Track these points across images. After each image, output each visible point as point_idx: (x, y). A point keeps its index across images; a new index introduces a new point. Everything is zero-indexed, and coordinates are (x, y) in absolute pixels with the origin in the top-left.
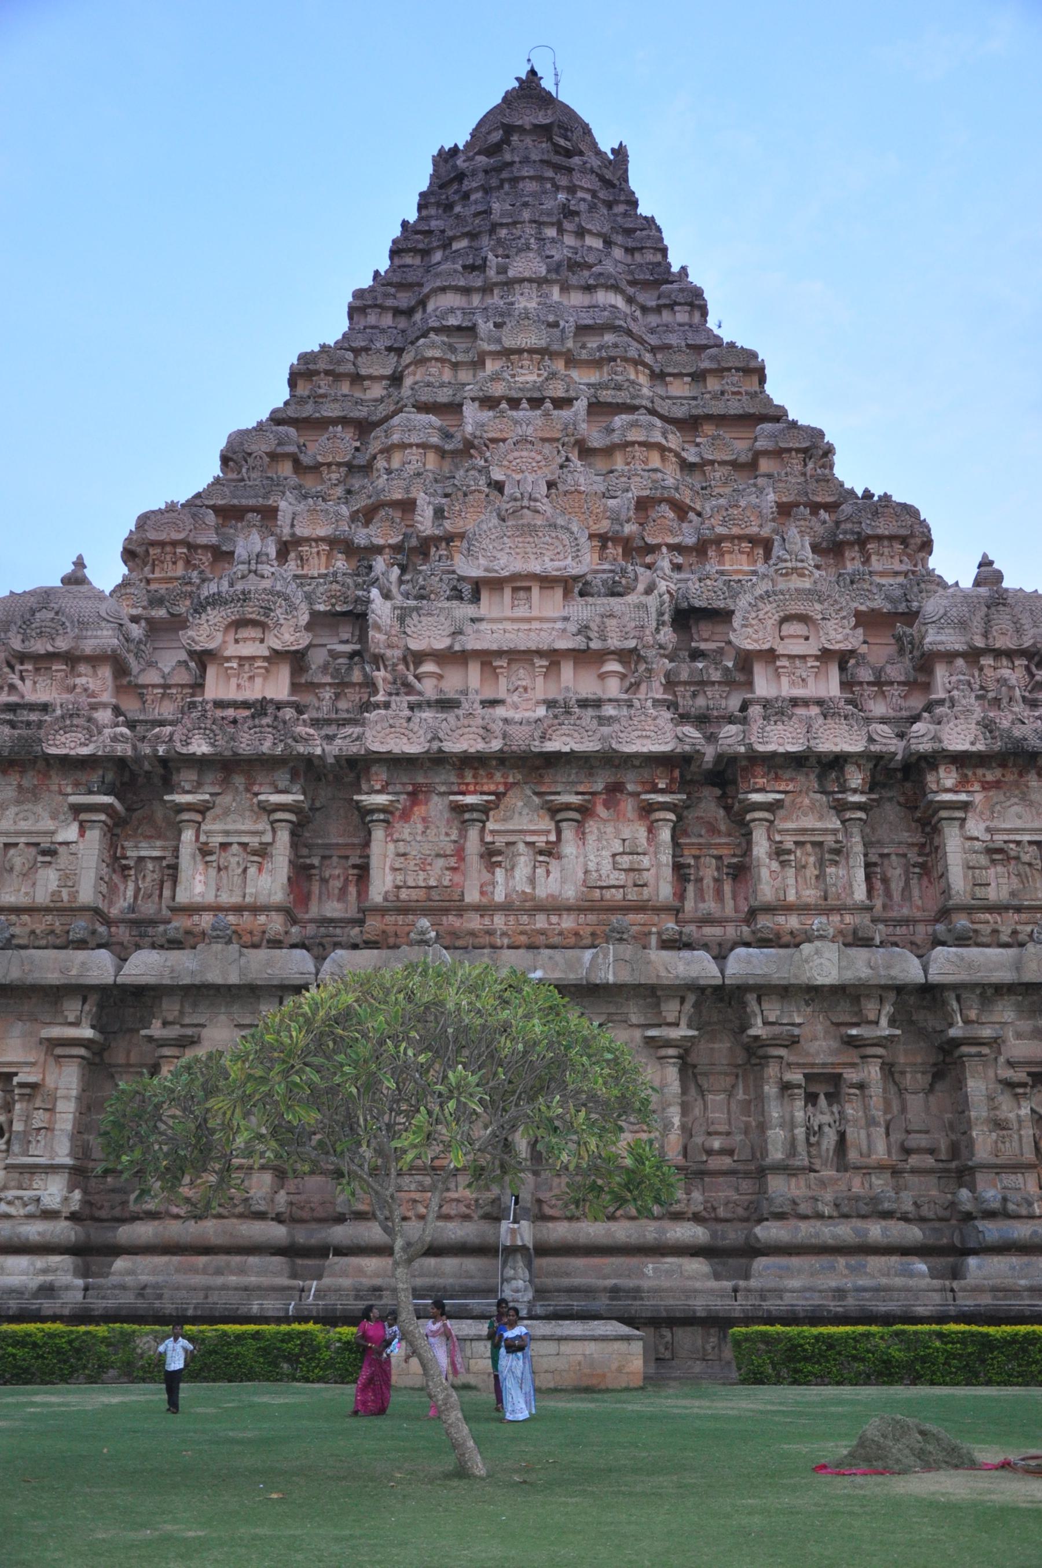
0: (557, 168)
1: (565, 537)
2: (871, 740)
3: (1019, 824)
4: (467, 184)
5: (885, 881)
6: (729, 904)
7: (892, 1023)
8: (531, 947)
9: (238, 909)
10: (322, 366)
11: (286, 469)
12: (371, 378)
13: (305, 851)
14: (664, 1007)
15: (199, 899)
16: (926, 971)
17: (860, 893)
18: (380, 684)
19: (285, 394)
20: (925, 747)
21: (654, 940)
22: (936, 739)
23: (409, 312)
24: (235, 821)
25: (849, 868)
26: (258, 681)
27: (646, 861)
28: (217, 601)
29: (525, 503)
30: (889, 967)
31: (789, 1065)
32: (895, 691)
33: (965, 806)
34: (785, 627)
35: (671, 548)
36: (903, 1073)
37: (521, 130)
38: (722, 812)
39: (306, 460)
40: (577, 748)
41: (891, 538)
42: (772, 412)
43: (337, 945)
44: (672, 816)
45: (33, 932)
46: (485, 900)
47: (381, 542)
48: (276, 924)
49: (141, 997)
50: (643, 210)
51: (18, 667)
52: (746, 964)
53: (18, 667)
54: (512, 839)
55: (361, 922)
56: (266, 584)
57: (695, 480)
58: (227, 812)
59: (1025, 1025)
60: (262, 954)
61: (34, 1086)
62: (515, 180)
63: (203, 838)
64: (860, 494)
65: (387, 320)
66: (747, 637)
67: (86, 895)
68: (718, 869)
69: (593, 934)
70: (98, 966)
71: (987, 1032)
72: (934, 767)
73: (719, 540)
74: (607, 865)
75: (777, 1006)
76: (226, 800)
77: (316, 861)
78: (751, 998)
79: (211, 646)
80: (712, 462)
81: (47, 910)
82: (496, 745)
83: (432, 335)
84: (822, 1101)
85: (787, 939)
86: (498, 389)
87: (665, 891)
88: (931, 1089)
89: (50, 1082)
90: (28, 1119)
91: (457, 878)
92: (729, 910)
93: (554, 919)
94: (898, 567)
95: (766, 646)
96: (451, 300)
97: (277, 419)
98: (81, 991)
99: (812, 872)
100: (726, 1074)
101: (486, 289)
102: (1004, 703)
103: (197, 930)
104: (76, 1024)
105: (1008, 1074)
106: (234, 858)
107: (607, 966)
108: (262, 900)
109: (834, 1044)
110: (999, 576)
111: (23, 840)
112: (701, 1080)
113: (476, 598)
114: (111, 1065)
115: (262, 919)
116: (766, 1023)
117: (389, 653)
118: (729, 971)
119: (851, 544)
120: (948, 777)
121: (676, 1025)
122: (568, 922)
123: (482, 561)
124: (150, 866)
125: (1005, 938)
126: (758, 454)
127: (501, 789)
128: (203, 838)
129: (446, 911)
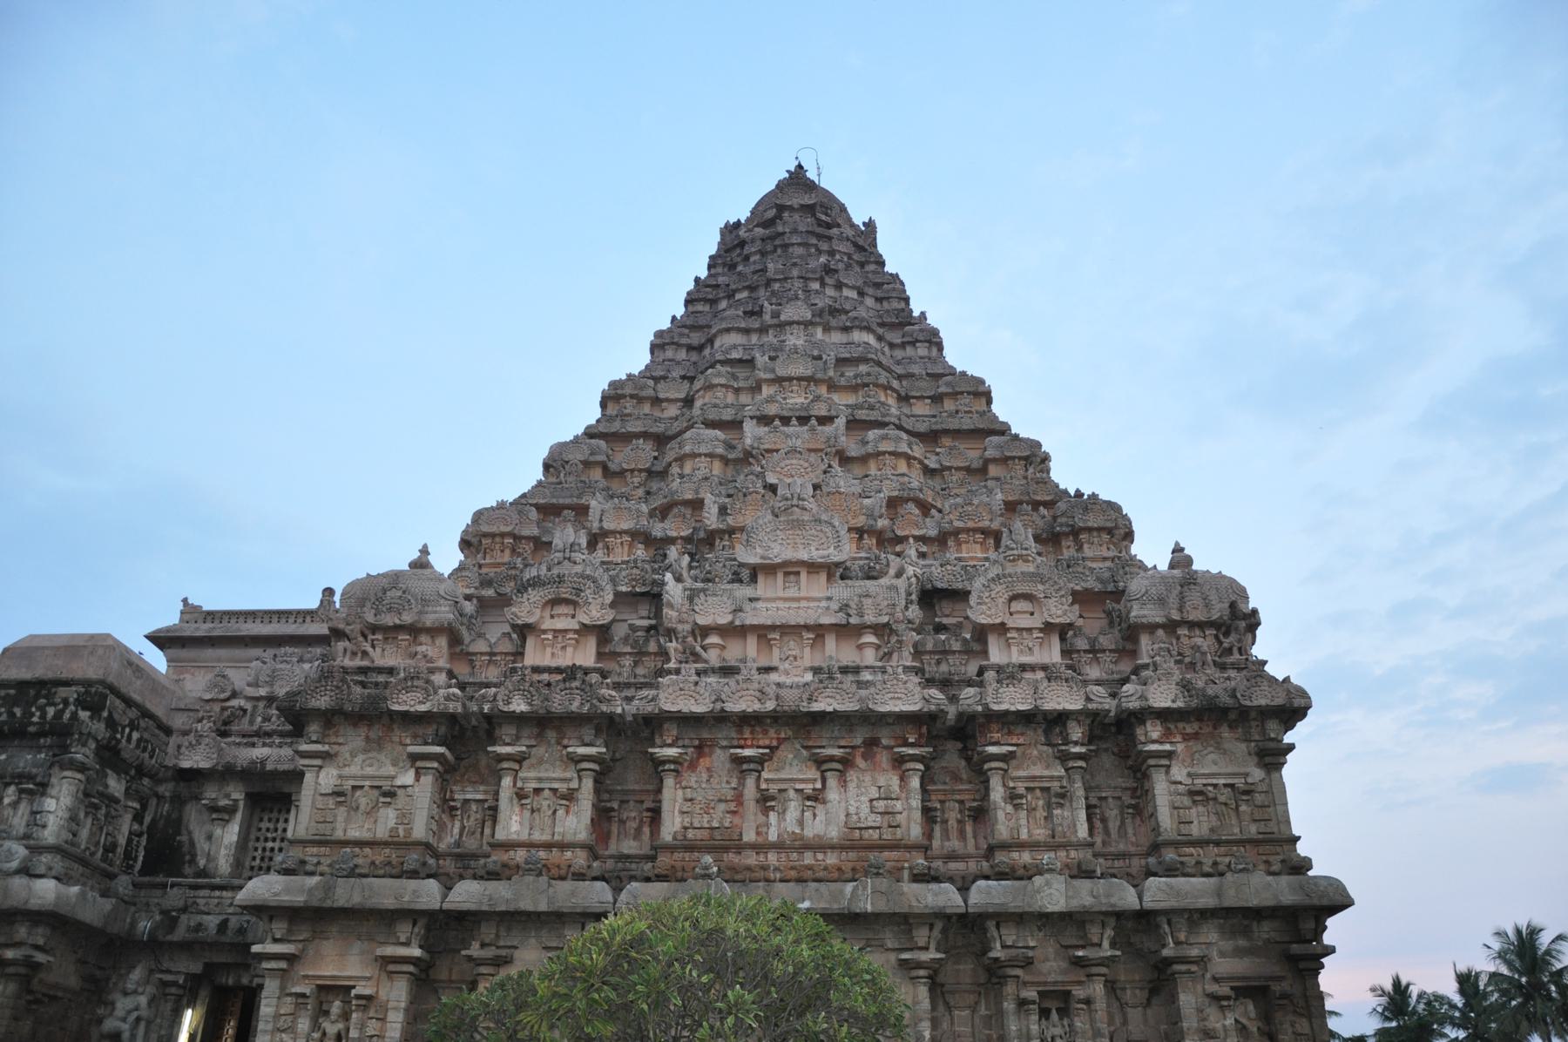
0: (819, 237)
1: (828, 530)
2: (1088, 699)
3: (1214, 769)
4: (747, 250)
5: (1104, 820)
6: (971, 841)
7: (1113, 945)
8: (800, 880)
9: (548, 846)
10: (628, 391)
11: (597, 474)
12: (668, 400)
13: (606, 796)
14: (915, 933)
15: (514, 837)
16: (1140, 898)
17: (1082, 832)
18: (672, 653)
19: (598, 413)
20: (1134, 704)
21: (906, 874)
22: (1143, 697)
23: (700, 348)
24: (546, 770)
25: (1073, 810)
26: (570, 650)
27: (899, 806)
28: (536, 583)
29: (795, 502)
30: (1108, 896)
31: (1025, 983)
32: (1106, 658)
33: (1169, 755)
34: (1014, 604)
35: (915, 537)
36: (1124, 989)
37: (791, 208)
38: (963, 763)
39: (613, 467)
40: (840, 708)
41: (1099, 529)
42: (997, 427)
43: (633, 878)
44: (921, 767)
45: (373, 863)
46: (760, 840)
47: (674, 534)
48: (580, 859)
49: (463, 921)
50: (889, 268)
51: (370, 637)
52: (986, 894)
53: (370, 637)
54: (783, 786)
55: (653, 858)
56: (578, 569)
57: (936, 483)
58: (541, 762)
59: (1228, 945)
60: (567, 886)
61: (369, 998)
62: (786, 246)
63: (519, 784)
64: (1072, 493)
65: (682, 354)
66: (981, 613)
67: (419, 831)
68: (961, 811)
69: (853, 869)
70: (428, 894)
71: (1194, 952)
72: (1143, 722)
73: (956, 532)
74: (865, 809)
75: (1014, 931)
76: (540, 751)
77: (615, 805)
78: (991, 924)
79: (531, 620)
80: (950, 468)
81: (386, 844)
82: (770, 705)
83: (718, 366)
84: (1054, 1016)
85: (1021, 872)
86: (772, 410)
87: (916, 832)
88: (1148, 1003)
89: (383, 995)
90: (362, 1027)
91: (737, 820)
92: (971, 849)
93: (820, 856)
94: (1106, 554)
95: (998, 621)
96: (734, 338)
97: (590, 433)
98: (412, 915)
99: (1041, 813)
100: (969, 992)
101: (763, 330)
102: (1199, 665)
103: (512, 863)
104: (407, 944)
105: (1213, 988)
106: (545, 802)
107: (865, 897)
108: (569, 838)
109: (1064, 965)
110: (1189, 561)
111: (367, 783)
112: (950, 998)
113: (753, 579)
114: (435, 981)
115: (569, 854)
116: (1004, 947)
117: (680, 627)
118: (971, 901)
119: (1067, 535)
120: (1154, 730)
121: (926, 949)
122: (832, 859)
123: (759, 550)
124: (474, 807)
125: (1207, 869)
126: (987, 462)
127: (775, 743)
128: (519, 784)
129: (726, 849)
